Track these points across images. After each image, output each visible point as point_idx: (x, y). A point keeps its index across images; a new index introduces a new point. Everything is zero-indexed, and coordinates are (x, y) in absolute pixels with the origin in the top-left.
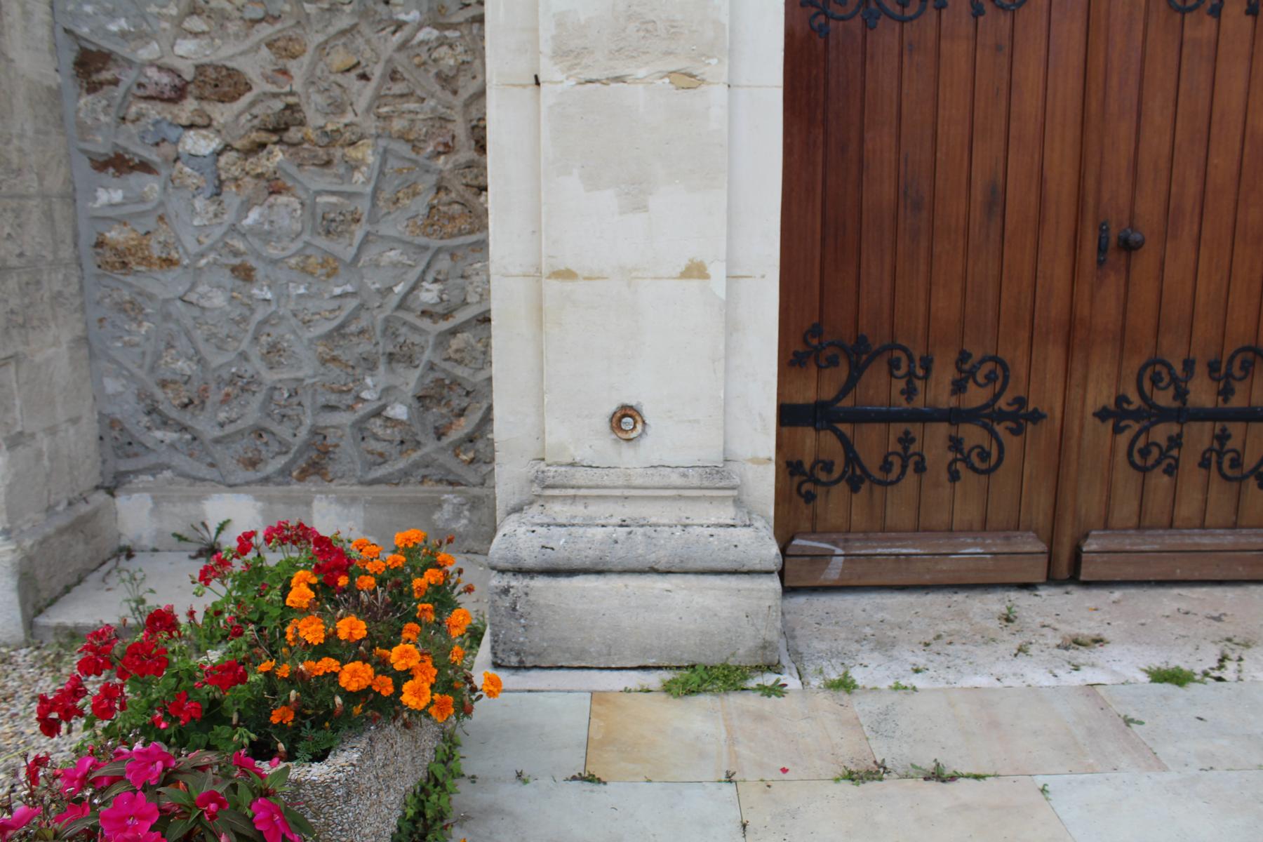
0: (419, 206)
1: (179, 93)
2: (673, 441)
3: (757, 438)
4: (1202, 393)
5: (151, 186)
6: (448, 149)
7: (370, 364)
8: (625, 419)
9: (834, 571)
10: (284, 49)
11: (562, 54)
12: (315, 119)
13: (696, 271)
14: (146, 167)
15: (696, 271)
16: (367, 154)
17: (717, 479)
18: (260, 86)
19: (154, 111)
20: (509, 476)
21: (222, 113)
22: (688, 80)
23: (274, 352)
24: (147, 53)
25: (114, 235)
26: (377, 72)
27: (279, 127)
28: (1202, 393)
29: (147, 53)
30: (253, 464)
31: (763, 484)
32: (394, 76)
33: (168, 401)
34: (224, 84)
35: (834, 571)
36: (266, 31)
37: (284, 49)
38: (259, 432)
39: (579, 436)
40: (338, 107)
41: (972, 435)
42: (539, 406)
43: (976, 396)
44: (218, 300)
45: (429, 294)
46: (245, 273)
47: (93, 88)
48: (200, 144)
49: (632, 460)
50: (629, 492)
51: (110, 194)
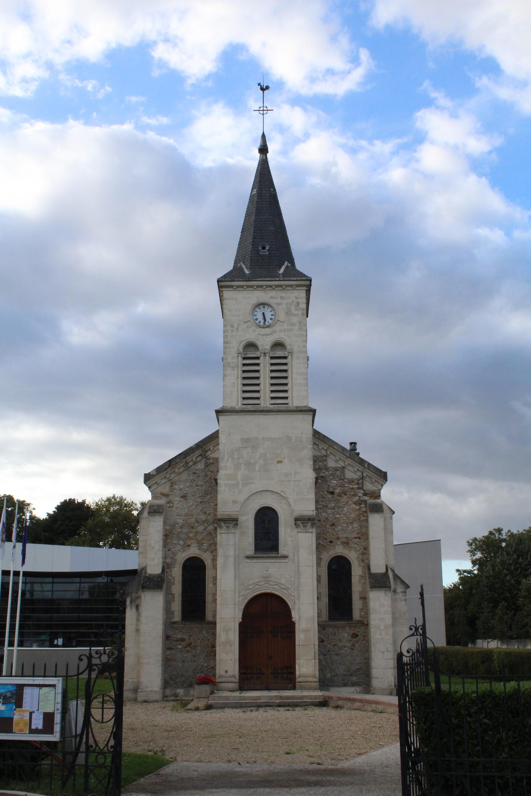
0: (205, 654)
1: (178, 641)
2: (230, 673)
3: (237, 673)
4: (280, 671)
5: (173, 651)
6: (208, 648)
7: (198, 673)
8: (226, 671)
9: (246, 688)
10: (190, 636)
11: (222, 644)
12: (193, 644)
13: (232, 660)
14: (173, 649)
15: (232, 660)
16: (199, 648)
17: (233, 676)
18: (187, 640)
19: (174, 643)
20: (217, 676)
21: (182, 643)
22: (231, 646)
23: (187, 671)
24: (174, 636)
25: (169, 657)
26: (201, 639)
27: (189, 645)
28: (280, 671)
29: (174, 636)
30: (183, 685)
31: (237, 677)
32: (202, 639)
33: (173, 677)
34: (183, 640)
35: (246, 688)
36: (189, 634)
37: (190, 636)
38: (184, 681)
39: (223, 673)
40: (196, 643)
41: (258, 675)
42: (220, 671)
43: (258, 672)
44: (180, 665)
45: (205, 665)
46: (184, 662)
47: (168, 640)
48: (180, 647)
49: (227, 675)
50: (227, 677)
51: (168, 652)
